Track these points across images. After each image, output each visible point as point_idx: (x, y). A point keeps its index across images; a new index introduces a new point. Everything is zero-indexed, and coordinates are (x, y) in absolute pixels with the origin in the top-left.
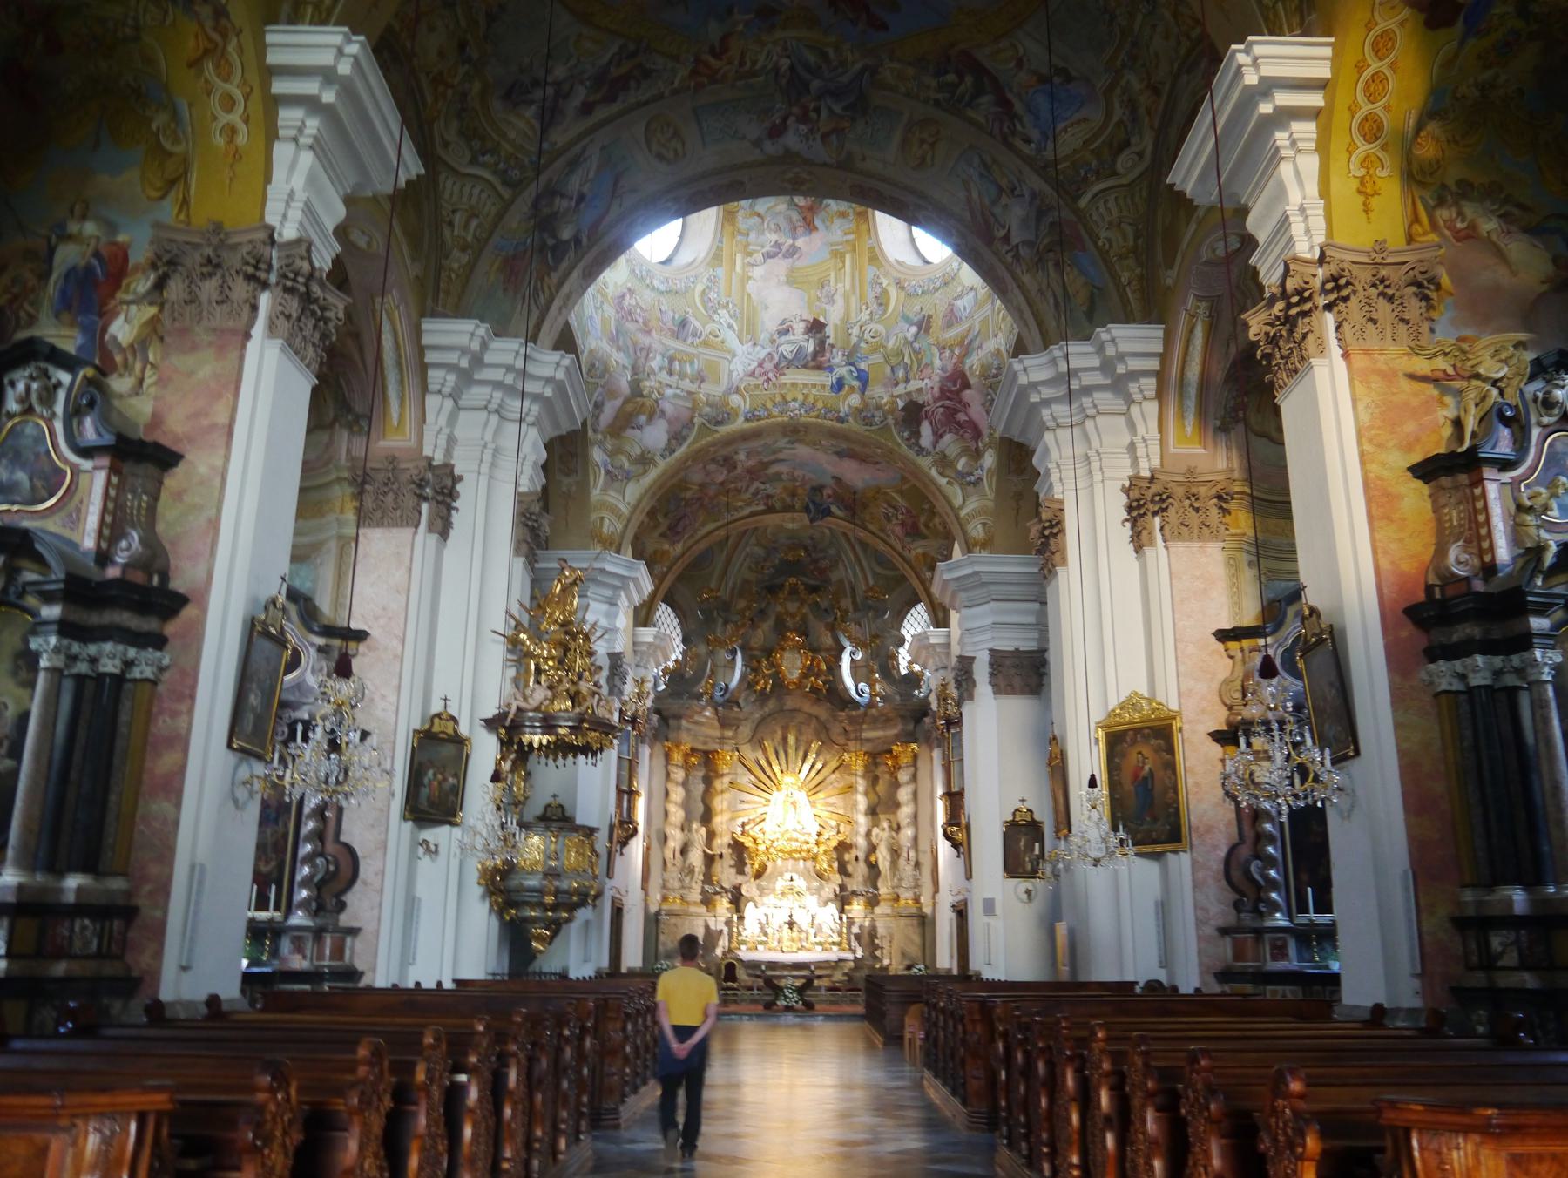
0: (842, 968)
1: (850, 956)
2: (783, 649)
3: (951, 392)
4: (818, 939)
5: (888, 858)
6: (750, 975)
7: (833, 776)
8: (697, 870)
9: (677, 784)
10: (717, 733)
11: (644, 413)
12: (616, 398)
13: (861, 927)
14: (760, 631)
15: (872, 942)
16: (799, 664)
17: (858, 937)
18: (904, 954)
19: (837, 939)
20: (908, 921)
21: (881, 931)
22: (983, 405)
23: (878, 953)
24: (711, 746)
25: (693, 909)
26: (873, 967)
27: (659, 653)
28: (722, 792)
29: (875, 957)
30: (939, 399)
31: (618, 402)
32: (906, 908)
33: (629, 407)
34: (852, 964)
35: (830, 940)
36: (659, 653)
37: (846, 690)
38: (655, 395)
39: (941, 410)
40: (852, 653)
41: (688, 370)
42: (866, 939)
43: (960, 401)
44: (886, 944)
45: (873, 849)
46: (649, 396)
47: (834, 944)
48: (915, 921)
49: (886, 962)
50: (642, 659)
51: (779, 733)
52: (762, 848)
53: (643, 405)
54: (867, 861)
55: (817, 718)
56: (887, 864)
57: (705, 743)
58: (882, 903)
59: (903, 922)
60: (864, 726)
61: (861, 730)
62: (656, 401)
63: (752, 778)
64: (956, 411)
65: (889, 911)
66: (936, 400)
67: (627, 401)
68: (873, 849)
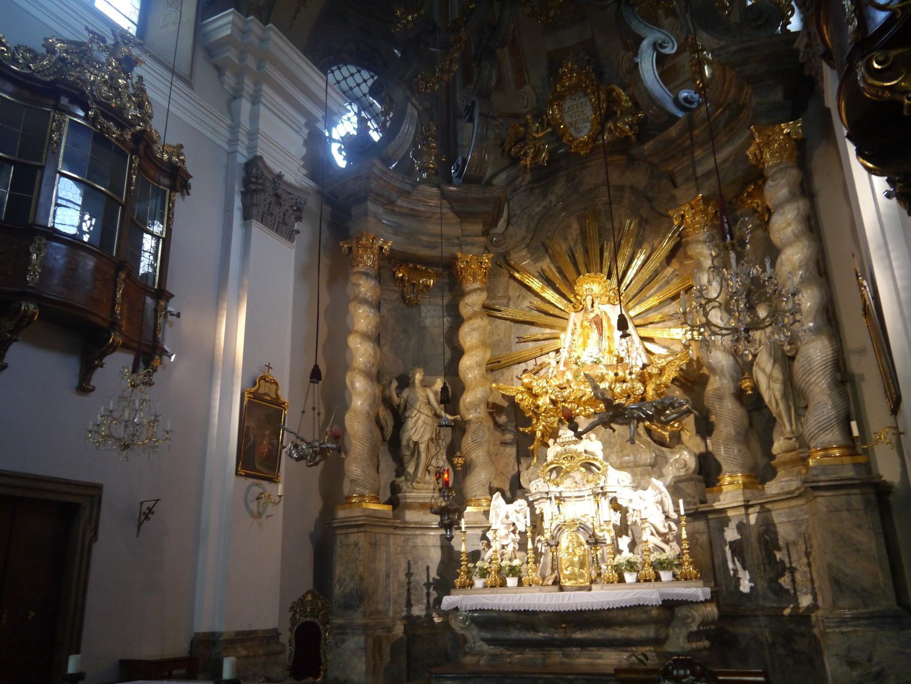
0: (684, 621)
1: (698, 591)
2: (560, 98)
4: (636, 558)
5: (777, 374)
6: (488, 641)
7: (669, 270)
8: (422, 447)
9: (364, 301)
10: (456, 231)
13: (741, 527)
14: (527, 88)
15: (770, 557)
16: (588, 111)
17: (738, 549)
18: (838, 583)
19: (671, 551)
20: (838, 499)
21: (785, 532)
23: (785, 581)
24: (447, 251)
25: (411, 516)
26: (777, 615)
27: (269, 69)
28: (470, 318)
29: (780, 591)
32: (824, 469)
34: (712, 610)
35: (654, 557)
36: (269, 69)
37: (652, 100)
40: (656, 46)
42: (755, 551)
44: (799, 561)
45: (744, 368)
47: (660, 565)
48: (856, 499)
49: (805, 601)
50: (240, 83)
51: (576, 226)
52: (544, 401)
54: (739, 395)
55: (633, 189)
56: (777, 387)
57: (432, 246)
58: (781, 472)
59: (823, 501)
60: (698, 153)
61: (694, 164)
63: (537, 302)
65: (795, 484)
68: (744, 368)
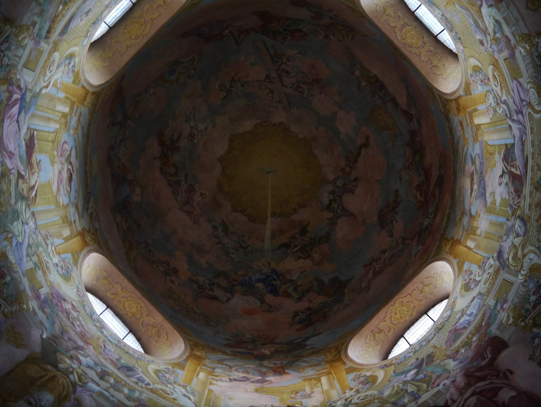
3: (480, 369)
11: (51, 391)
12: (18, 347)
22: (531, 358)
30: (468, 385)
31: (21, 354)
33: (33, 371)
38: (74, 377)
39: (473, 400)
41: (126, 391)
43: (497, 373)
46: (67, 373)
53: (54, 378)
62: (74, 385)
64: (496, 390)
66: (461, 391)
67: (31, 359)
